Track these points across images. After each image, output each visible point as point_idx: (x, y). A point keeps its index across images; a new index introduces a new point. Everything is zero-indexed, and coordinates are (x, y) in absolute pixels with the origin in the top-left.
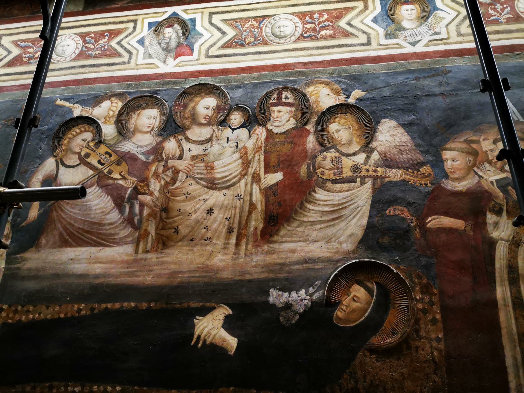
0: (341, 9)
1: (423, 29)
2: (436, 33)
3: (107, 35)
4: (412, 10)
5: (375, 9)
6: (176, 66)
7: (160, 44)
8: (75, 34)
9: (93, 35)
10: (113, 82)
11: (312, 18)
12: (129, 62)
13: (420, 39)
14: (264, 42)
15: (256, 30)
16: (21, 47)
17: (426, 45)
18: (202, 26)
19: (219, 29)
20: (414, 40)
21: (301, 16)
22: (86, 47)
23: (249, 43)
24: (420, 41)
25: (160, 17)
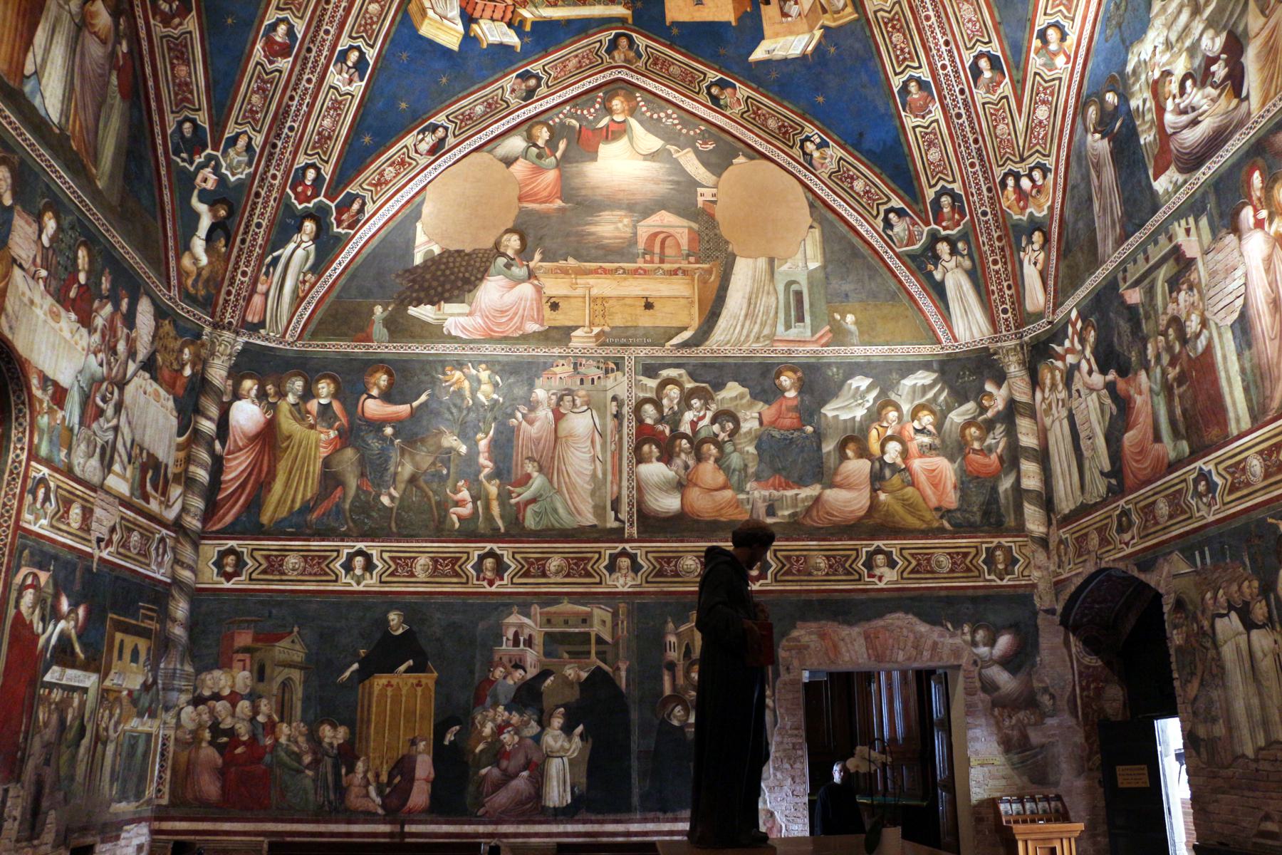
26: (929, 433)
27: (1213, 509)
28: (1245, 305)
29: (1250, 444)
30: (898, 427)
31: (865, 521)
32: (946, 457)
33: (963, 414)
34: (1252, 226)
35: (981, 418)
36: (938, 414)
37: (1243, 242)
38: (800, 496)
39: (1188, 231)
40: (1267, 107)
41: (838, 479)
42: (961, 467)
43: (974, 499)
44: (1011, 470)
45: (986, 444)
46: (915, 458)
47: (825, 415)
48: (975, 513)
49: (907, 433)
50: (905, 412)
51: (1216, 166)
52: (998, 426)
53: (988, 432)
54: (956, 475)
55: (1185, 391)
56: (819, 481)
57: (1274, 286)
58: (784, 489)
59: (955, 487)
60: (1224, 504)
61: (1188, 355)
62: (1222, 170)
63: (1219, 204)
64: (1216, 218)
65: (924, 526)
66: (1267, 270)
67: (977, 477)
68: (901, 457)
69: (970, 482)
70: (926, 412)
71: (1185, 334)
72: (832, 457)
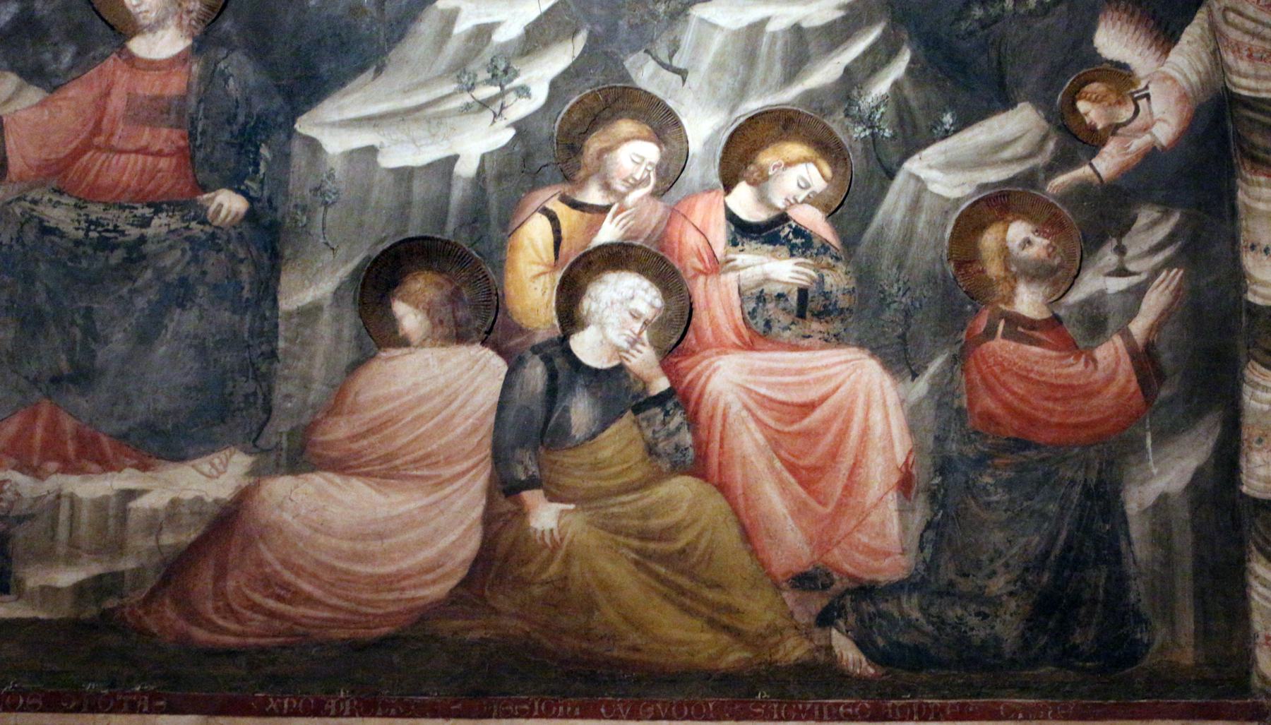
26: (802, 242)
30: (655, 213)
31: (447, 627)
32: (875, 352)
33: (980, 160)
35: (1062, 180)
36: (856, 160)
38: (143, 503)
41: (339, 431)
42: (941, 395)
43: (998, 537)
44: (1194, 416)
45: (1077, 296)
46: (723, 347)
47: (313, 146)
48: (995, 602)
49: (692, 240)
50: (695, 146)
52: (1145, 216)
53: (1092, 241)
54: (912, 430)
56: (252, 443)
58: (68, 467)
59: (905, 485)
65: (735, 656)
67: (1021, 444)
68: (656, 344)
69: (981, 462)
70: (795, 149)
72: (325, 328)
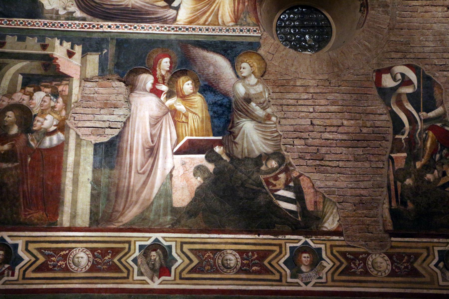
0: (266, 250)
1: (312, 274)
2: (320, 278)
3: (110, 252)
4: (308, 257)
5: (286, 254)
6: (160, 284)
7: (148, 264)
8: (86, 248)
9: (99, 251)
10: (117, 293)
11: (247, 255)
12: (127, 278)
13: (310, 280)
14: (217, 271)
15: (212, 260)
16: (45, 254)
17: (314, 286)
18: (176, 253)
19: (188, 257)
20: (307, 281)
21: (241, 252)
22: (96, 261)
23: (208, 270)
24: (310, 282)
25: (147, 241)
27: (6, 278)
28: (120, 136)
29: (81, 239)
34: (148, 90)
37: (133, 94)
39: (70, 54)
40: (194, 27)
51: (126, 30)
55: (11, 169)
57: (156, 139)
60: (24, 278)
61: (28, 143)
62: (131, 36)
63: (118, 55)
64: (110, 65)
66: (153, 126)
71: (32, 125)
